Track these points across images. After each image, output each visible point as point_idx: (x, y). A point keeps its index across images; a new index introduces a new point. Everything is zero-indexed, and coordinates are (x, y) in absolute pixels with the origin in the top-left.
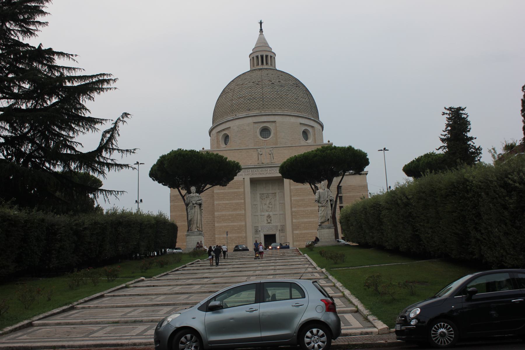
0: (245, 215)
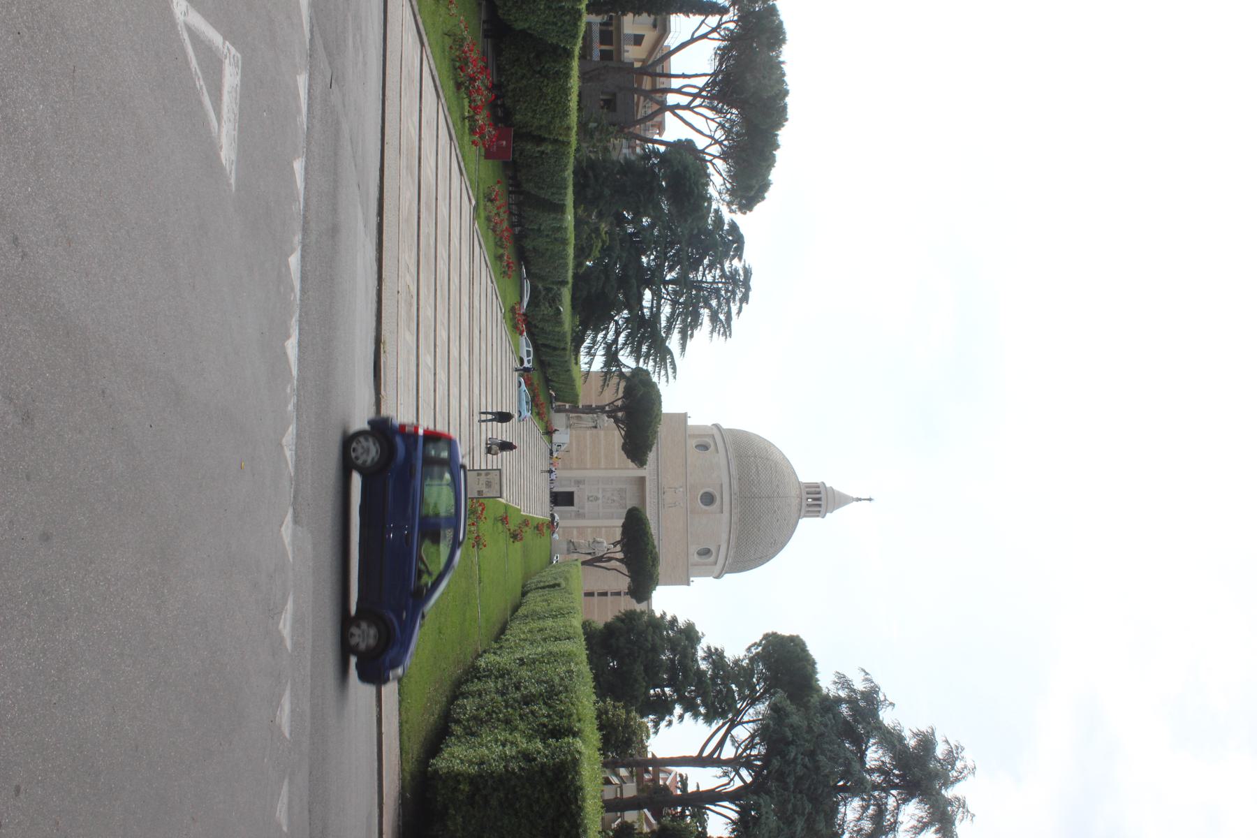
0: (599, 469)
